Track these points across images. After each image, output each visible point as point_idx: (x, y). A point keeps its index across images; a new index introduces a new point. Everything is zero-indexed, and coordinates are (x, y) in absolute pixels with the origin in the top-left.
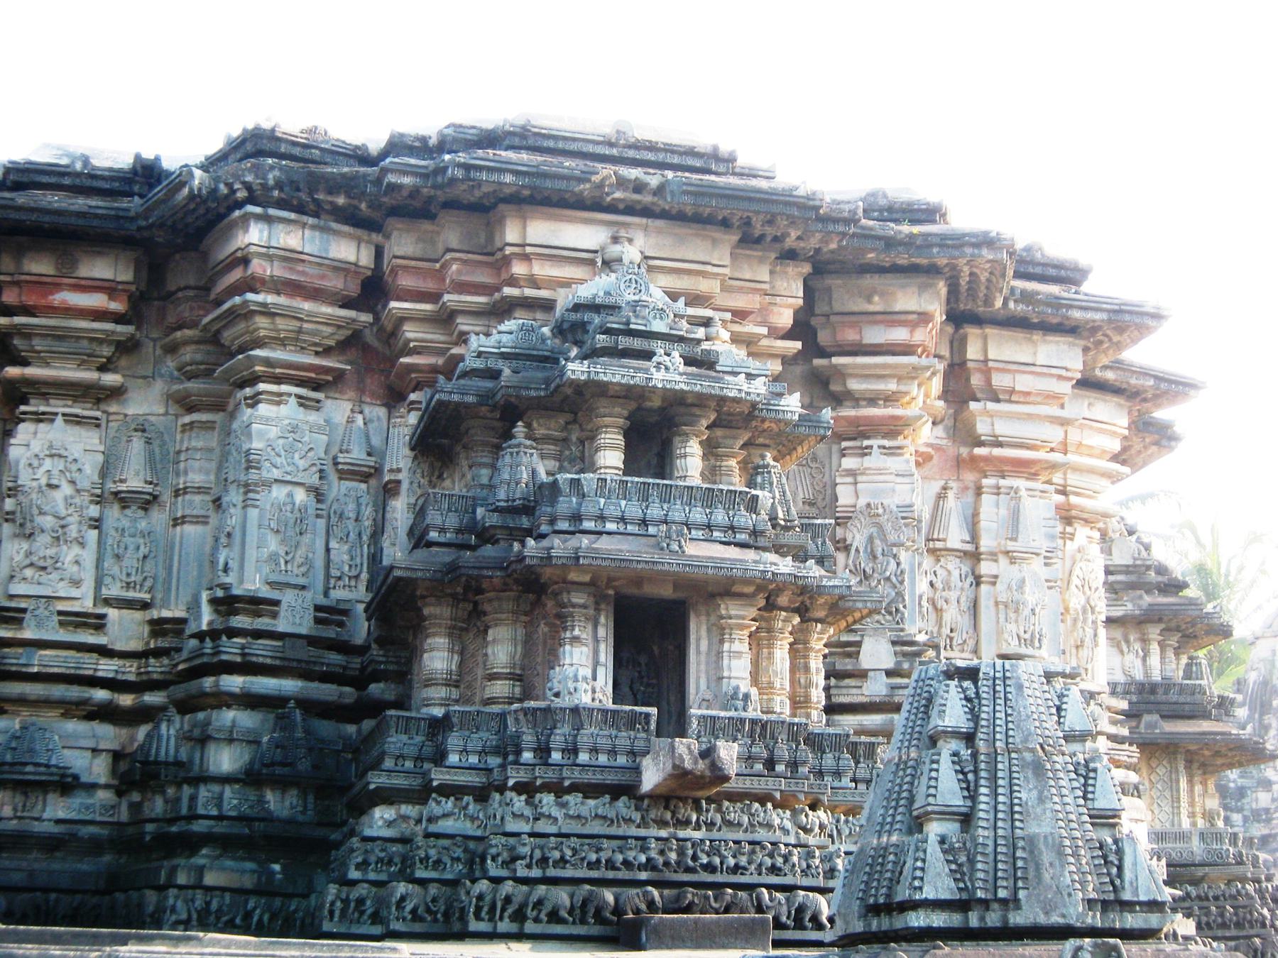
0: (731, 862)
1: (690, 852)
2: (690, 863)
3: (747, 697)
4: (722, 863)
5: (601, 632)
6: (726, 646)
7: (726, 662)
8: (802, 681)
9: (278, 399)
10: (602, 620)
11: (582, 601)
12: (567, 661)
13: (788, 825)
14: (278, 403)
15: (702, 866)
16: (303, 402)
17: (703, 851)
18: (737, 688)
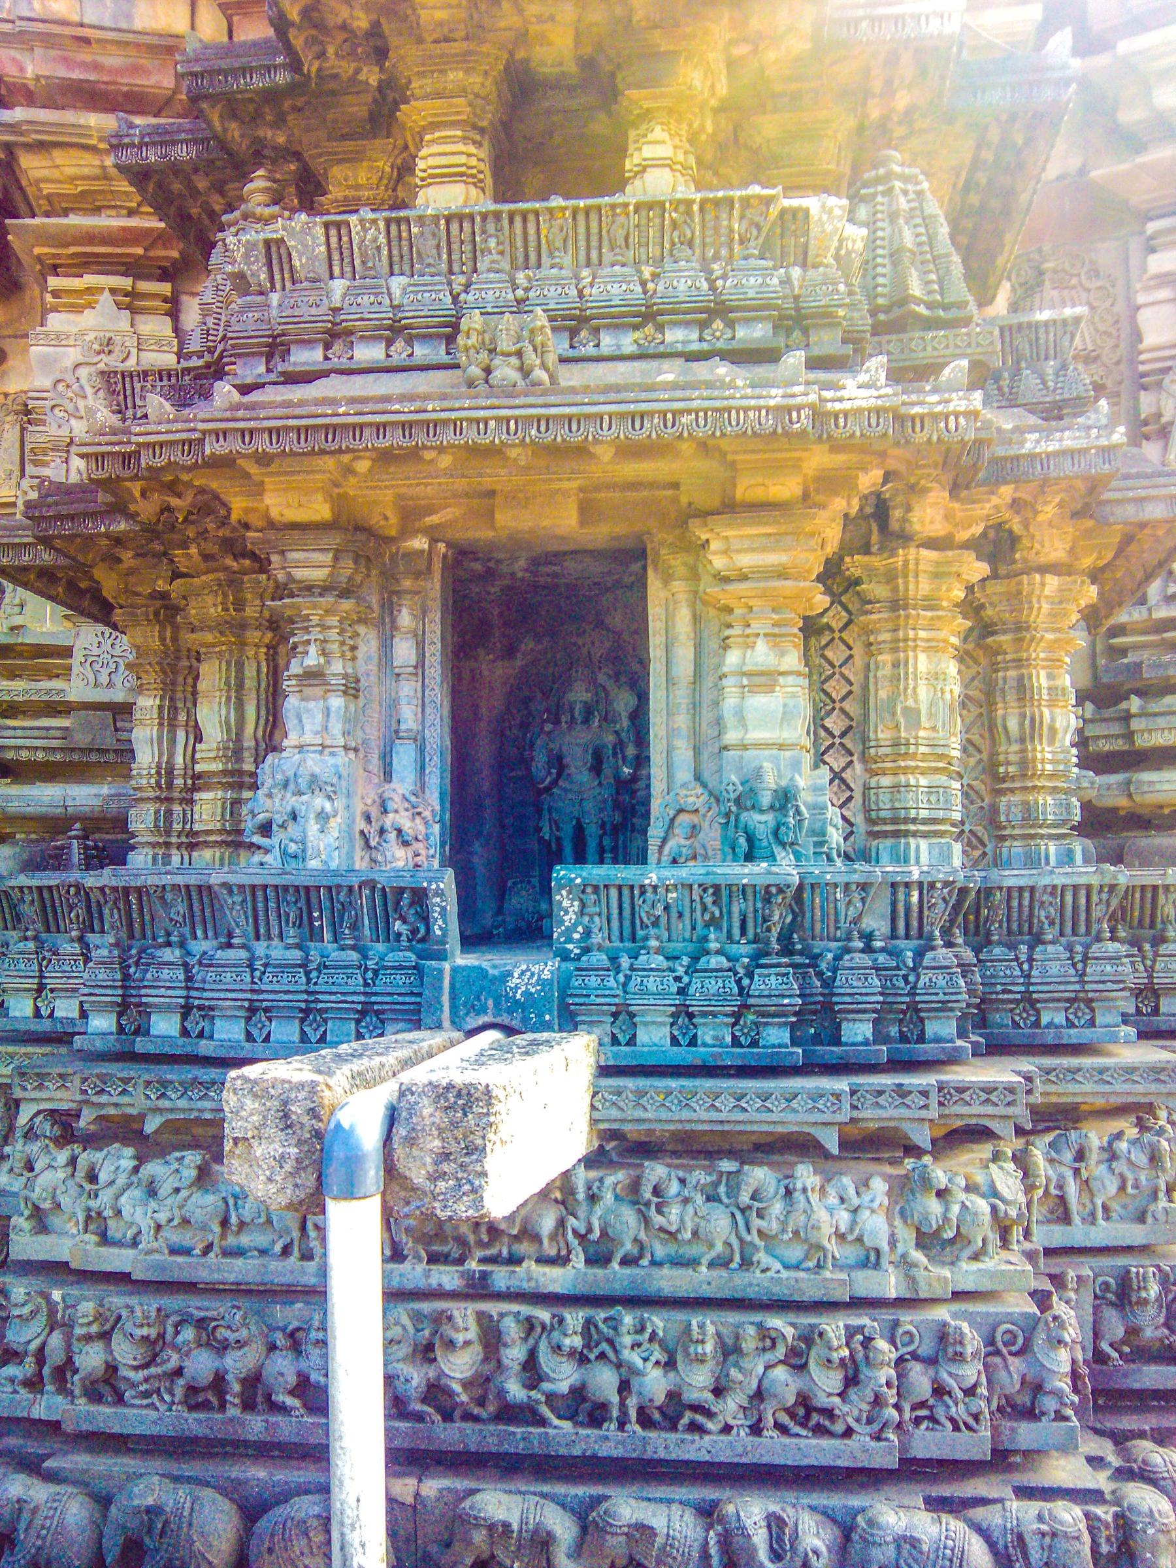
0: (655, 1384)
1: (514, 1354)
2: (515, 1390)
3: (785, 799)
4: (624, 1387)
5: (404, 651)
6: (732, 658)
7: (730, 701)
8: (1013, 724)
9: (83, 301)
10: (405, 619)
11: (319, 574)
12: (292, 739)
13: (876, 1226)
14: (77, 309)
15: (550, 1398)
16: (131, 303)
17: (557, 1349)
18: (758, 773)
